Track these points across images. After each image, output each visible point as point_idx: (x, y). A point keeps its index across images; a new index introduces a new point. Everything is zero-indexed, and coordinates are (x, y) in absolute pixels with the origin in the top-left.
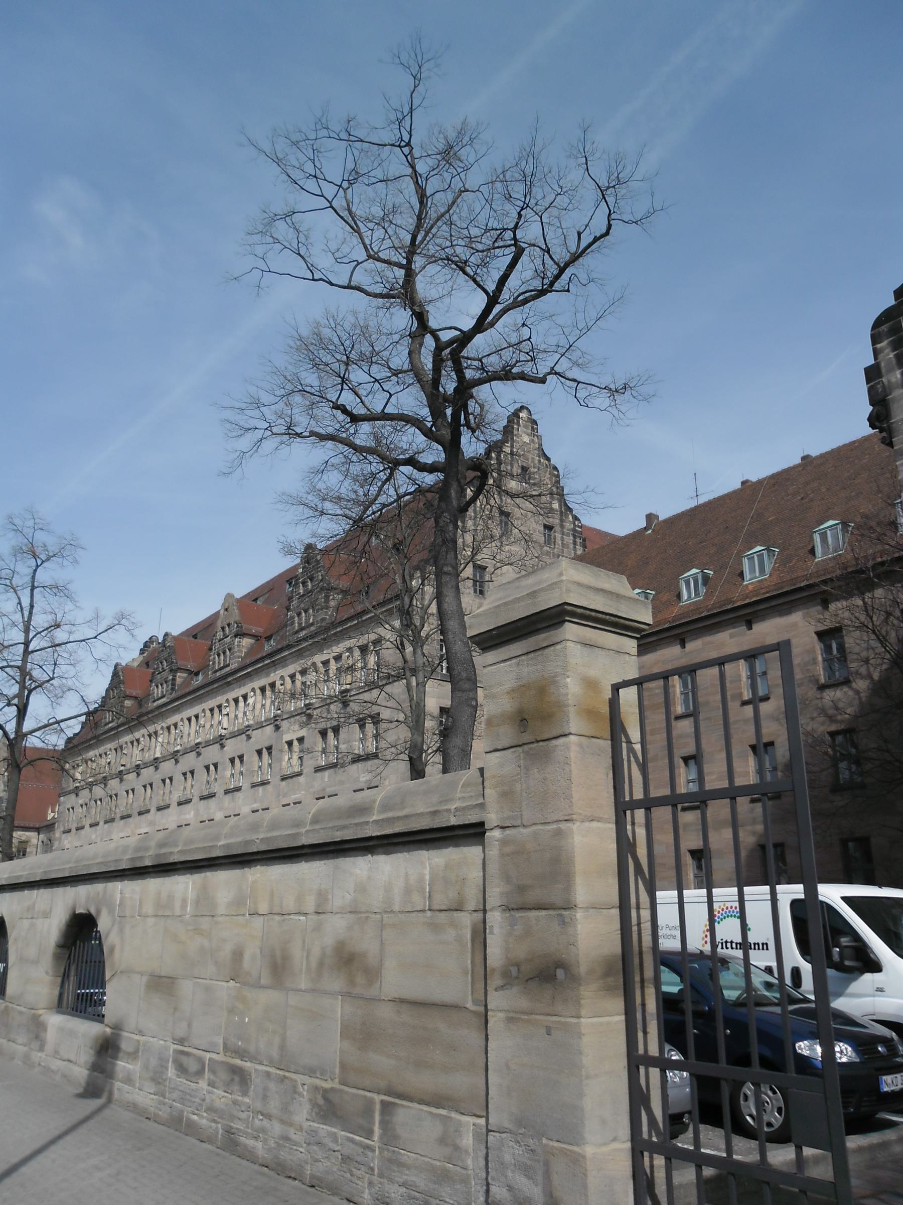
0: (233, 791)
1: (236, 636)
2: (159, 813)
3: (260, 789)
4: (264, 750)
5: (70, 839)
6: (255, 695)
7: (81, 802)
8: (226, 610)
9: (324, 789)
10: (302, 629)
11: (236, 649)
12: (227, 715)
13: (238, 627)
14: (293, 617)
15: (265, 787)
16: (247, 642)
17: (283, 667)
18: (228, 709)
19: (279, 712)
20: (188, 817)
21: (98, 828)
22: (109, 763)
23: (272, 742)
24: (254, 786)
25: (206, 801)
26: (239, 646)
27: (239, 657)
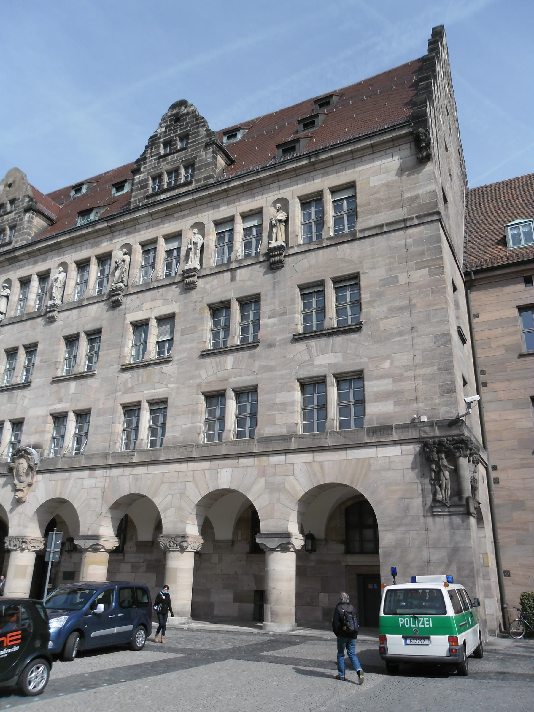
0: (12, 389)
1: (27, 210)
3: (73, 385)
4: (83, 336)
6: (66, 271)
8: (10, 186)
9: (225, 380)
10: (164, 191)
11: (26, 225)
12: (7, 297)
13: (31, 200)
14: (147, 180)
15: (83, 381)
16: (38, 222)
17: (128, 233)
18: (8, 291)
19: (121, 285)
23: (104, 324)
24: (57, 380)
26: (30, 222)
27: (29, 234)
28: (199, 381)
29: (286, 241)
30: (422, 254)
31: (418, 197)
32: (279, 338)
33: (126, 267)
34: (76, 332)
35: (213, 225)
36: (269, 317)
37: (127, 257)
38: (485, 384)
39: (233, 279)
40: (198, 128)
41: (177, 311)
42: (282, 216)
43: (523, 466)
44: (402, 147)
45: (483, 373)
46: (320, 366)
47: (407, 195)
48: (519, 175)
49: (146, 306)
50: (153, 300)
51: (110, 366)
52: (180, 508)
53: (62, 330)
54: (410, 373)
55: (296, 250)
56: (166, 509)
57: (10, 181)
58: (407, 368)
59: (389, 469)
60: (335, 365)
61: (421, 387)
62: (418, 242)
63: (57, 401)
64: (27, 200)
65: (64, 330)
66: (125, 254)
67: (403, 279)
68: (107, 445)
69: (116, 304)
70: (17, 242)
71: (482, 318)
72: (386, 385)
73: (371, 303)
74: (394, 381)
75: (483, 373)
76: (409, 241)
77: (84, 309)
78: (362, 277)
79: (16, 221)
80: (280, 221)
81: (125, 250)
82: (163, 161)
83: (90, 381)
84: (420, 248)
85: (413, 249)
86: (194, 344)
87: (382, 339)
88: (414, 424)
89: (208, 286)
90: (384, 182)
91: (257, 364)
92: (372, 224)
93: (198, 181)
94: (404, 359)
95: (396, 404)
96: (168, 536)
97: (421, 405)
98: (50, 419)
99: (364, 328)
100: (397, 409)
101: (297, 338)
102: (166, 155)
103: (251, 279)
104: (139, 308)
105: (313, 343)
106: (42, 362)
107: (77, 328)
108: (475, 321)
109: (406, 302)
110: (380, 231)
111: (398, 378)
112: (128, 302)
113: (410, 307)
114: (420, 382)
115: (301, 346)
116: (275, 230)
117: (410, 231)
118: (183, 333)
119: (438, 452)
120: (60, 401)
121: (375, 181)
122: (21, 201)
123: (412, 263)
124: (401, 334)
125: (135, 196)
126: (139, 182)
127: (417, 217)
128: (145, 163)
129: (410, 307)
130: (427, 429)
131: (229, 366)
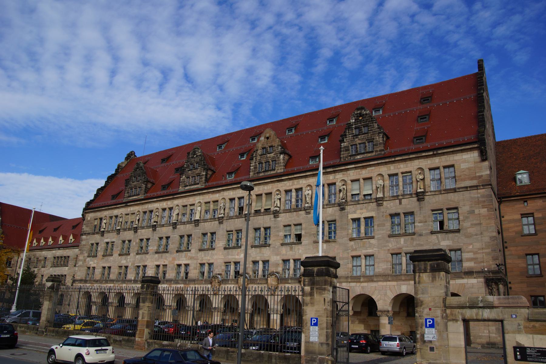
2: (203, 253)
5: (96, 261)
9: (400, 248)
14: (348, 147)
15: (330, 244)
19: (344, 200)
20: (237, 257)
21: (129, 257)
22: (139, 220)
23: (337, 218)
25: (258, 249)
28: (388, 248)
29: (424, 189)
30: (484, 202)
31: (482, 176)
32: (424, 232)
33: (345, 192)
35: (387, 176)
36: (419, 223)
37: (344, 187)
38: (506, 248)
39: (400, 203)
40: (373, 123)
41: (374, 215)
42: (421, 177)
43: (521, 283)
44: (475, 152)
45: (506, 242)
46: (443, 245)
47: (477, 174)
48: (521, 137)
49: (358, 211)
50: (361, 209)
52: (385, 300)
54: (479, 251)
55: (429, 194)
56: (378, 301)
58: (479, 249)
59: (473, 288)
60: (449, 246)
61: (485, 257)
62: (483, 196)
64: (280, 147)
66: (344, 185)
67: (477, 211)
68: (347, 273)
69: (343, 209)
70: (278, 170)
71: (506, 218)
72: (471, 255)
73: (463, 221)
74: (474, 254)
75: (506, 242)
76: (479, 195)
78: (459, 209)
80: (421, 179)
81: (343, 183)
82: (357, 138)
84: (484, 199)
85: (481, 199)
86: (384, 232)
87: (469, 236)
88: (482, 272)
89: (388, 206)
90: (467, 167)
91: (415, 243)
92: (463, 186)
93: (376, 151)
94: (478, 245)
95: (475, 263)
96: (380, 311)
97: (485, 264)
99: (461, 231)
100: (475, 265)
101: (432, 233)
102: (356, 135)
103: (410, 204)
104: (355, 212)
105: (439, 235)
106: (305, 233)
108: (502, 219)
109: (478, 222)
110: (466, 188)
111: (475, 253)
112: (348, 208)
113: (480, 224)
114: (484, 255)
115: (434, 237)
116: (419, 183)
117: (479, 191)
118: (378, 226)
119: (492, 282)
121: (464, 166)
123: (480, 205)
124: (476, 235)
125: (343, 155)
126: (345, 147)
127: (482, 185)
128: (346, 138)
129: (480, 224)
130: (487, 274)
131: (402, 242)
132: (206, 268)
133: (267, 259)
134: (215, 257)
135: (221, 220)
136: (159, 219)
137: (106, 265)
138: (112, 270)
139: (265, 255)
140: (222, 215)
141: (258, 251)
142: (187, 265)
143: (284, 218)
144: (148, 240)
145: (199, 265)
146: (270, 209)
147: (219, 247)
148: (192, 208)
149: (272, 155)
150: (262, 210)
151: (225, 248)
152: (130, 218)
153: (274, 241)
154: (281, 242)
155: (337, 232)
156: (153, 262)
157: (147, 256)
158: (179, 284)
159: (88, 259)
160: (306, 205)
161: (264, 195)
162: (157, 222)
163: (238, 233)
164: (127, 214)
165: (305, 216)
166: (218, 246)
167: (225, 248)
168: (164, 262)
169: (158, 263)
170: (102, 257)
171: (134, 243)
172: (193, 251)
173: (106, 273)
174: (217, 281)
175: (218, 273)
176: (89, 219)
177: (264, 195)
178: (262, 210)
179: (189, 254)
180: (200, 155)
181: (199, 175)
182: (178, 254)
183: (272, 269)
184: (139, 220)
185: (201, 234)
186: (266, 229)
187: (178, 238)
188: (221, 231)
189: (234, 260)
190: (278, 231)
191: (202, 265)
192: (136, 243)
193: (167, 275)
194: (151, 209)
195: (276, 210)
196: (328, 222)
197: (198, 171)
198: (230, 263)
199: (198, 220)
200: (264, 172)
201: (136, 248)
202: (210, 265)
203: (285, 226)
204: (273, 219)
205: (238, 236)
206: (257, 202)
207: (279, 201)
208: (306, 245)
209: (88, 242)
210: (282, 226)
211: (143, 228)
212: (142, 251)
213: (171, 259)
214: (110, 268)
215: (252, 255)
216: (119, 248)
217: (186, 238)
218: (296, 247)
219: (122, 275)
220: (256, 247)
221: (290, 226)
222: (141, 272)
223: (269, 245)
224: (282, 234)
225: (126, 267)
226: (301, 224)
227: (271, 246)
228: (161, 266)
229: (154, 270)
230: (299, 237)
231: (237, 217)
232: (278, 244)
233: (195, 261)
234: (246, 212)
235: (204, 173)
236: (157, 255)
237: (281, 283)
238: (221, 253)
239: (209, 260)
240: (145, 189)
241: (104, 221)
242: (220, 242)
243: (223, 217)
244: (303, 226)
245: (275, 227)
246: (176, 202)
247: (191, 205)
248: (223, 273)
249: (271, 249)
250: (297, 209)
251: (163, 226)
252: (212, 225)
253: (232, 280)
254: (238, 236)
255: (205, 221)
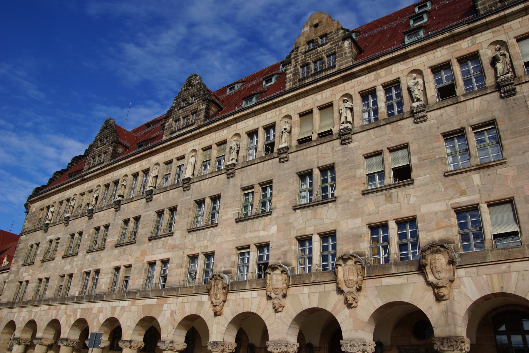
2: (195, 235)
5: (31, 271)
7: (50, 237)
20: (262, 233)
21: (76, 259)
22: (97, 198)
25: (309, 212)
34: (459, 127)
51: (524, 153)
53: (438, 128)
57: (316, 22)
63: (458, 194)
65: (441, 128)
70: (341, 65)
77: (460, 104)
79: (335, 49)
83: (500, 170)
98: (453, 213)
106: (420, 160)
107: (459, 123)
120: (463, 193)
122: (335, 34)
132: (201, 262)
133: (331, 228)
134: (218, 240)
135: (230, 172)
136: (127, 190)
137: (43, 276)
138: (50, 283)
139: (326, 221)
140: (234, 161)
141: (309, 216)
142: (165, 262)
143: (362, 143)
144: (107, 227)
145: (187, 259)
146: (331, 130)
147: (227, 220)
148: (180, 163)
149: (328, 46)
150: (315, 137)
151: (238, 220)
152: (86, 199)
153: (345, 188)
154: (363, 188)
155: (504, 142)
156: (110, 262)
157: (102, 253)
158: (149, 298)
159: (23, 269)
160: (415, 105)
161: (316, 111)
162: (123, 196)
163: (264, 189)
164: (82, 194)
165: (415, 126)
166: (224, 217)
167: (238, 220)
168: (128, 260)
169: (116, 264)
170: (40, 264)
171: (87, 235)
172: (177, 234)
173: (42, 289)
174: (220, 286)
175: (223, 269)
176: (34, 210)
177: (316, 111)
178: (315, 137)
179: (170, 242)
180: (198, 84)
181: (195, 112)
182: (150, 244)
183: (343, 247)
184: (97, 198)
185: (193, 202)
186: (324, 170)
187: (154, 216)
188: (231, 191)
189: (256, 241)
190: (354, 168)
191: (193, 258)
192: (89, 236)
193: (130, 283)
194: (116, 179)
195: (346, 129)
196: (474, 128)
197: (194, 106)
198: (248, 247)
199: (189, 179)
200: (312, 75)
201: (88, 243)
202: (209, 256)
203: (367, 157)
204: (341, 147)
205: (265, 196)
206: (301, 127)
207: (349, 111)
208: (426, 184)
209: (27, 244)
210: (362, 158)
211: (101, 209)
212: (97, 247)
213: (138, 254)
214: (48, 279)
215: (295, 224)
216: (65, 247)
217: (167, 215)
218: (400, 193)
219: (63, 291)
220: (303, 207)
221: (379, 153)
222: (90, 283)
223: (334, 200)
224: (363, 172)
225: (71, 276)
226: (405, 146)
227: (339, 201)
228: (122, 268)
229: (110, 276)
230: (403, 174)
231: (263, 160)
232: (356, 193)
233: (181, 253)
234: (283, 145)
235: (204, 106)
236: (117, 251)
237: (370, 277)
238: (229, 231)
239: (206, 247)
240: (113, 154)
241: (51, 209)
242: (229, 210)
243: (234, 165)
244: (413, 147)
245: (344, 163)
246: (155, 159)
247: (179, 159)
248: (234, 270)
249: (340, 206)
250: (392, 118)
251: (131, 200)
252: (215, 183)
253: (251, 282)
254: (265, 196)
255: (202, 178)
